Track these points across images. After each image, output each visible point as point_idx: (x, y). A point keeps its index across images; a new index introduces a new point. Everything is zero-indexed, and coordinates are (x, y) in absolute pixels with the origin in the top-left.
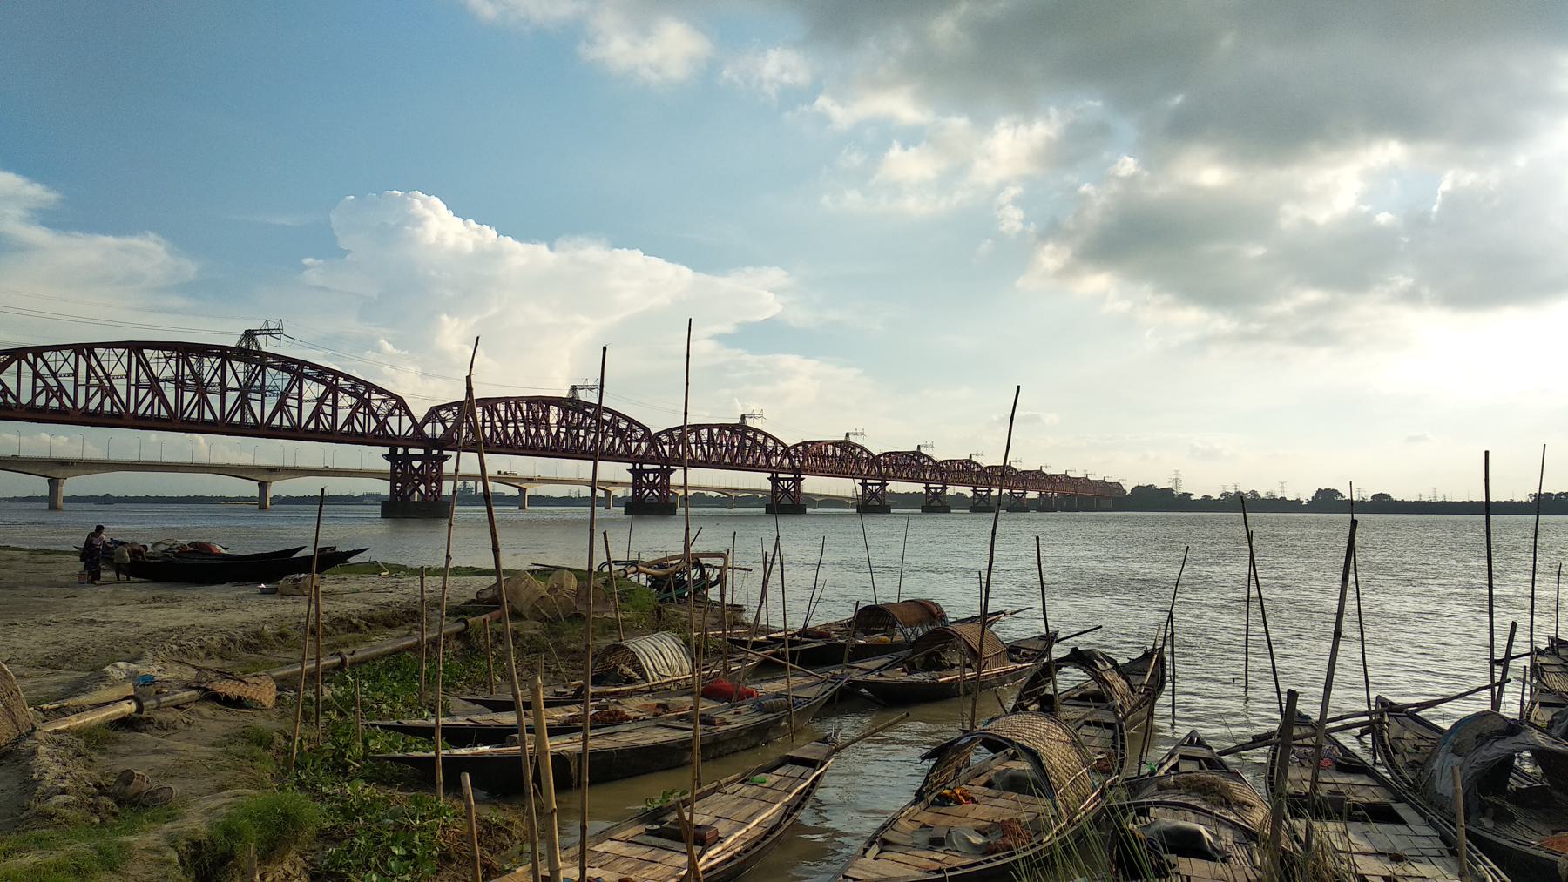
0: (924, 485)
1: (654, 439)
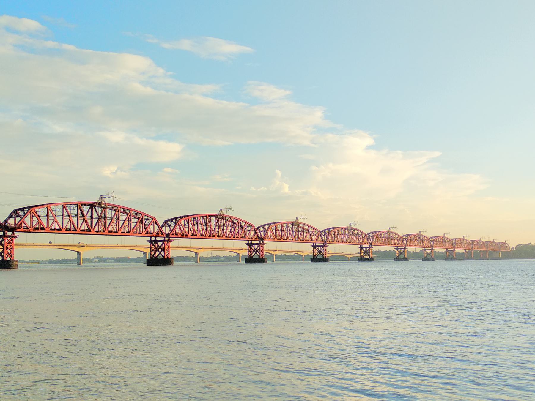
0: (395, 247)
1: (256, 230)
